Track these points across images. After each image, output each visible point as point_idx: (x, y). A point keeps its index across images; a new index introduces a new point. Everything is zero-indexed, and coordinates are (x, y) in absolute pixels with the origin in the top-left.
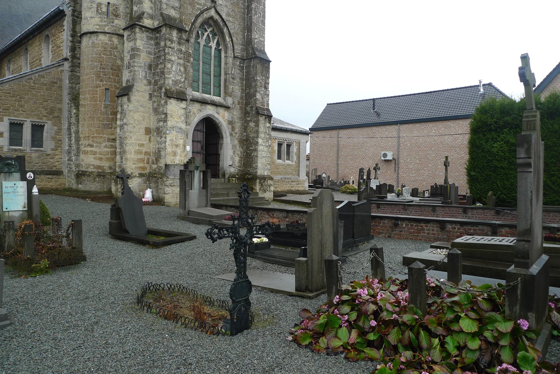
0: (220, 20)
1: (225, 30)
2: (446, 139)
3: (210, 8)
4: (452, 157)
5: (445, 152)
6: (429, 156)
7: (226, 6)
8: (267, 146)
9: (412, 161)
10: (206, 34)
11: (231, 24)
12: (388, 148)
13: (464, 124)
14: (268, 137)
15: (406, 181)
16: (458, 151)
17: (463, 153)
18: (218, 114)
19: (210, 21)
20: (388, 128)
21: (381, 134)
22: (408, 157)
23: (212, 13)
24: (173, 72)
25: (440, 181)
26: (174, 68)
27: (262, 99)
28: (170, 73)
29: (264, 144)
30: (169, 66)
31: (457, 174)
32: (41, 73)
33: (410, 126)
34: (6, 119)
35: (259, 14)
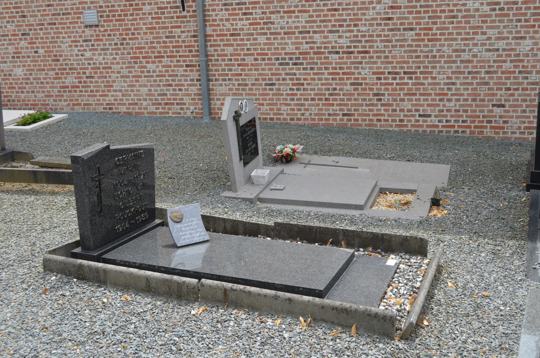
15: (249, 60)
25: (465, 56)
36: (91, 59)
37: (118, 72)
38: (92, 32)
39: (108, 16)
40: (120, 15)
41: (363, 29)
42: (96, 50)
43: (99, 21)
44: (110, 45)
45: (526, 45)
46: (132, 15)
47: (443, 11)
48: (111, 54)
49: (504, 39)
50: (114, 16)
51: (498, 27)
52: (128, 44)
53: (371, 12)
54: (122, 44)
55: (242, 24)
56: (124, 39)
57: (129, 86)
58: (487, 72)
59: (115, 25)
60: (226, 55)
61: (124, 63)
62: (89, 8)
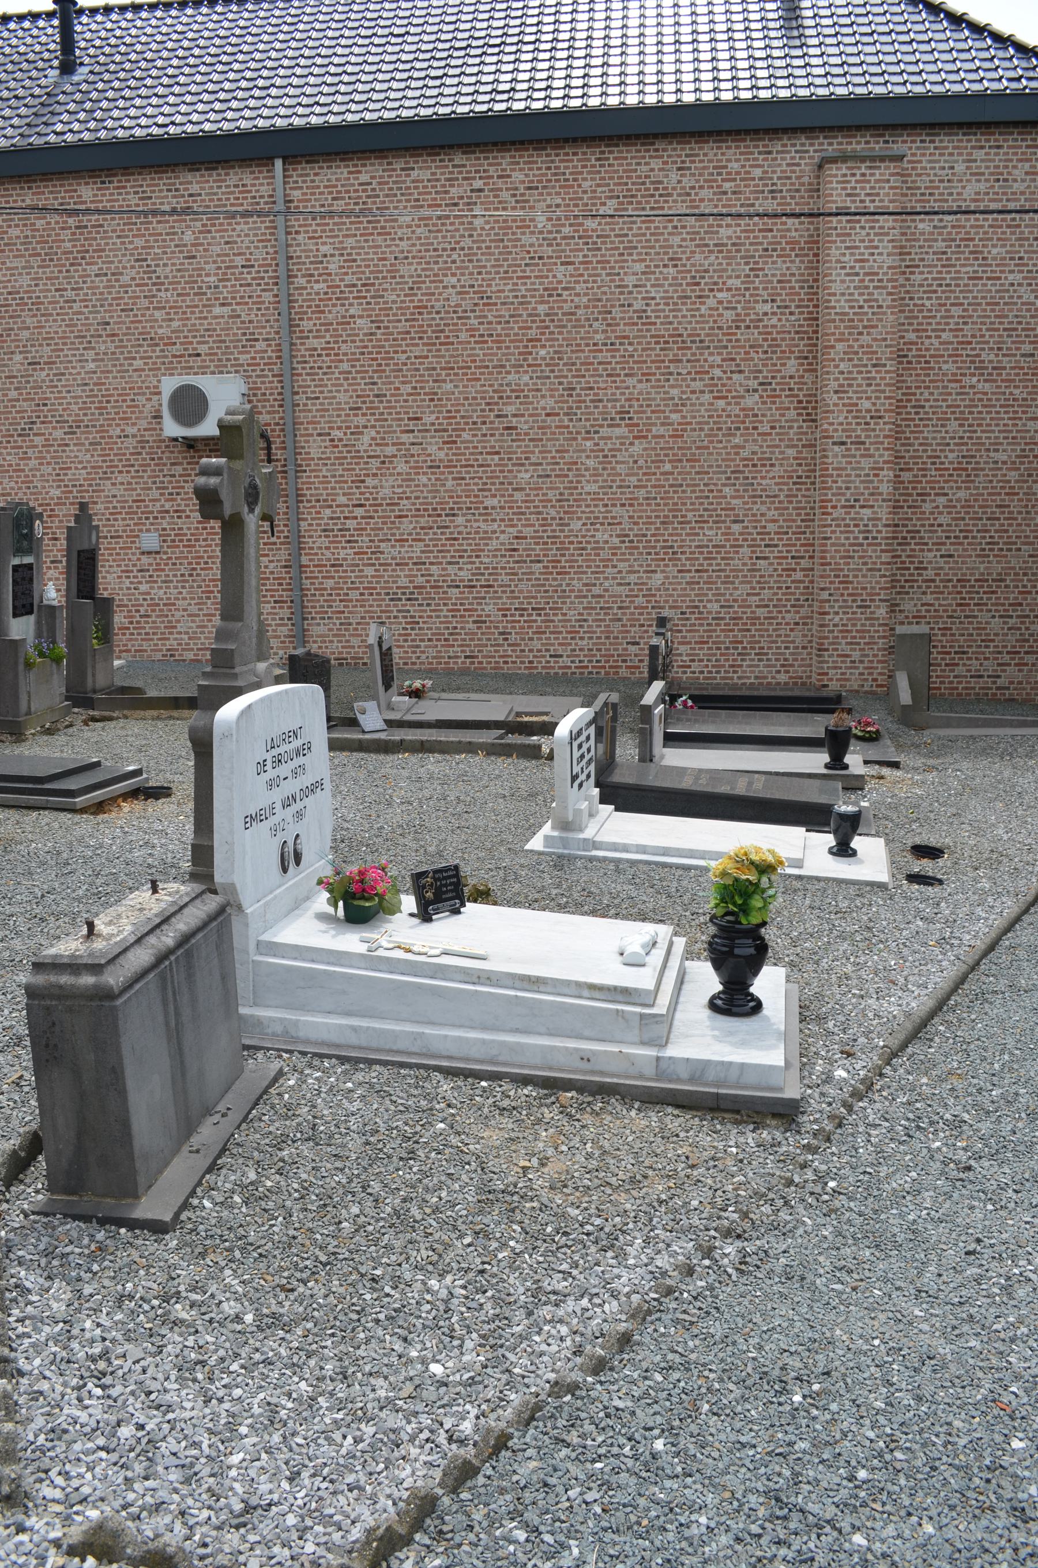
2: (630, 280)
4: (674, 417)
5: (631, 381)
6: (510, 410)
9: (390, 450)
12: (203, 349)
13: (758, 172)
15: (354, 595)
16: (717, 372)
17: (753, 384)
20: (195, 188)
21: (139, 242)
22: (361, 420)
25: (596, 590)
31: (711, 534)
33: (364, 178)
36: (149, 593)
37: (185, 610)
38: (151, 561)
39: (174, 541)
40: (189, 540)
41: (486, 560)
42: (156, 582)
43: (161, 547)
44: (175, 576)
45: (658, 579)
46: (205, 540)
47: (571, 543)
48: (176, 588)
49: (635, 572)
50: (181, 541)
51: (628, 560)
52: (198, 575)
53: (494, 542)
54: (191, 575)
55: (345, 553)
56: (194, 569)
57: (198, 627)
58: (620, 608)
59: (182, 552)
60: (325, 589)
61: (193, 599)
62: (149, 531)
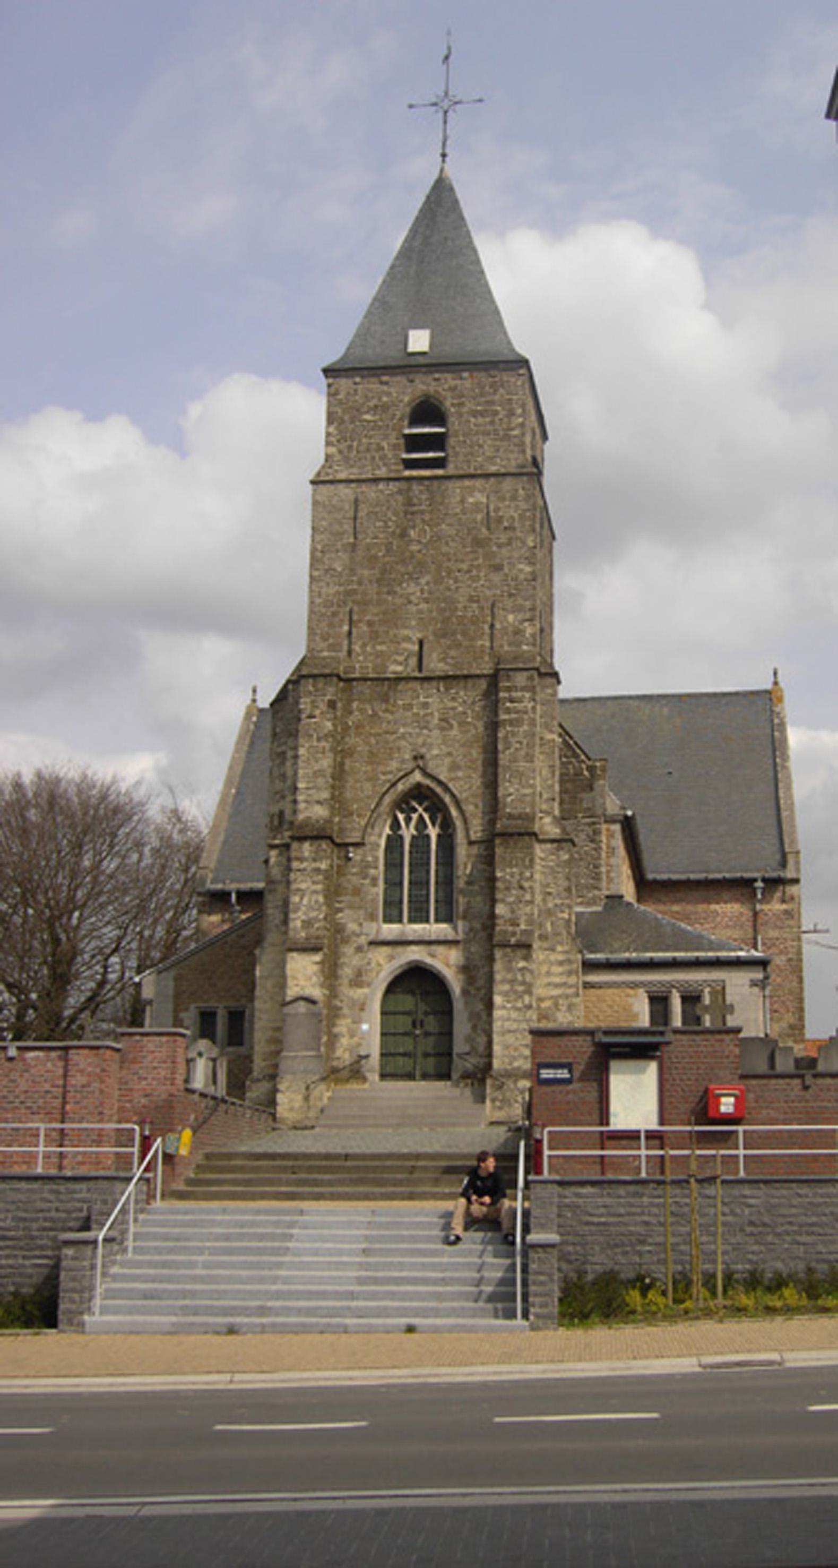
0: (433, 785)
1: (447, 799)
3: (412, 771)
7: (450, 754)
8: (519, 1009)
10: (415, 816)
11: (462, 783)
14: (521, 988)
18: (433, 956)
19: (419, 793)
23: (418, 777)
24: (303, 909)
26: (305, 901)
27: (513, 912)
28: (297, 910)
29: (509, 1005)
30: (295, 899)
32: (240, 932)
34: (192, 1007)
35: (518, 746)
